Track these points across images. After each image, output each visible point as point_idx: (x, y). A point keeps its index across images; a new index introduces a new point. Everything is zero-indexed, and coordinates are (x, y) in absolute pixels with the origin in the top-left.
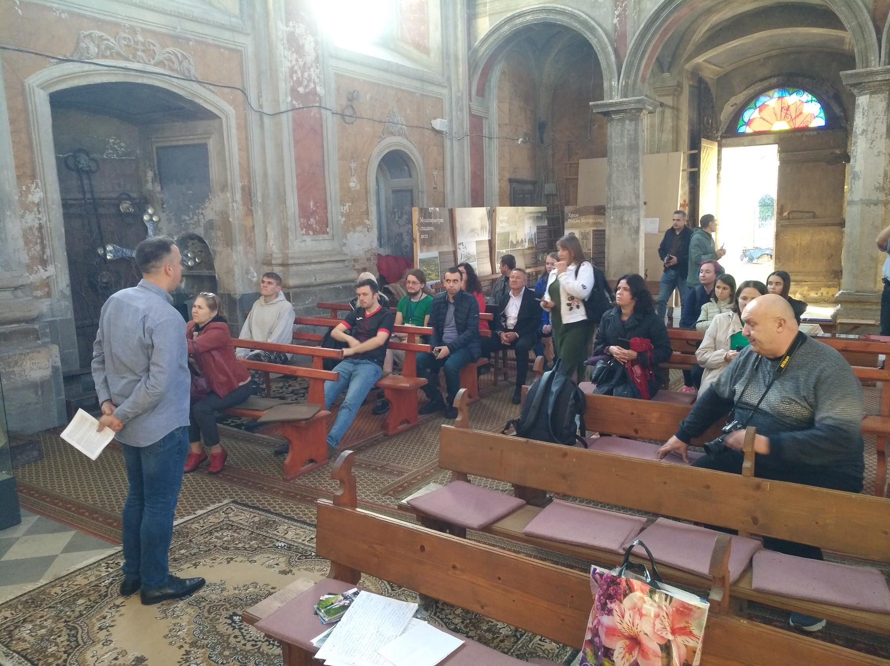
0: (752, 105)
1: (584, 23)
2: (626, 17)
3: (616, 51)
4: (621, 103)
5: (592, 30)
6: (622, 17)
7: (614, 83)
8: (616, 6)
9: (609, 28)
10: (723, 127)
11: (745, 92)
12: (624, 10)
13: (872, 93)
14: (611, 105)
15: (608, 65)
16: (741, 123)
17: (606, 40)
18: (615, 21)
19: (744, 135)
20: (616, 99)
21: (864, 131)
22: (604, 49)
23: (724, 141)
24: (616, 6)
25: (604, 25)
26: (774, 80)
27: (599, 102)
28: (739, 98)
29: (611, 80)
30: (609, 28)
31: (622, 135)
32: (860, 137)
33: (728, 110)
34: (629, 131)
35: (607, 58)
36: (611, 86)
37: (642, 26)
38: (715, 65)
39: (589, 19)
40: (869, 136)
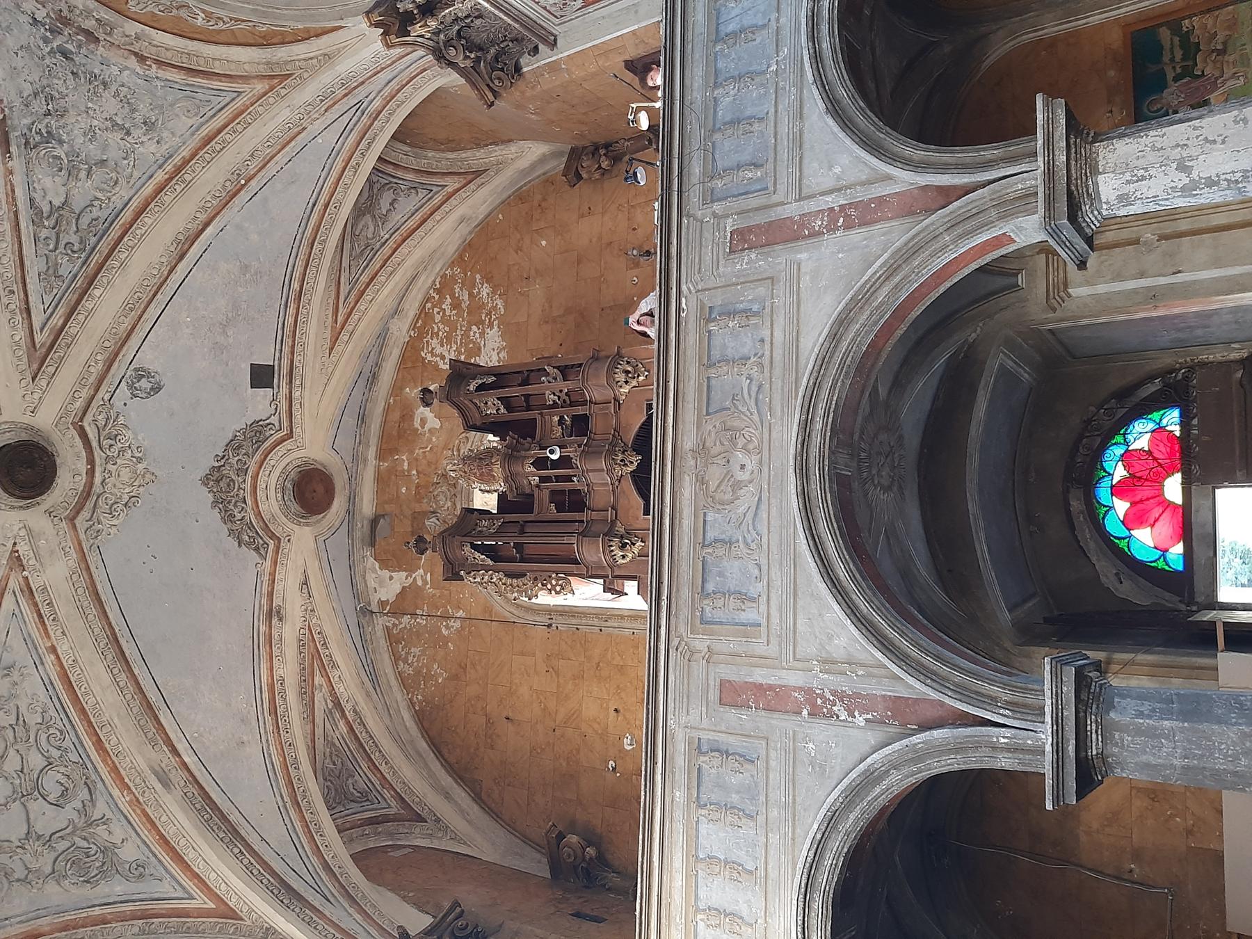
0: (1123, 544)
1: (854, 794)
2: (857, 695)
3: (925, 727)
4: (1058, 722)
5: (870, 779)
6: (854, 703)
7: (1002, 737)
8: (831, 715)
9: (872, 737)
10: (1169, 600)
11: (1094, 559)
12: (840, 696)
13: (1095, 171)
14: (1059, 748)
15: (957, 750)
16: (1161, 564)
17: (897, 746)
18: (860, 720)
19: (1188, 555)
20: (1045, 735)
21: (1183, 168)
22: (918, 756)
23: (1200, 599)
24: (831, 715)
25: (866, 748)
26: (1076, 505)
27: (1049, 782)
28: (1106, 570)
29: (995, 747)
30: (872, 737)
31: (1152, 733)
32: (1195, 175)
33: (1129, 590)
34: (1140, 714)
35: (944, 752)
36: (1011, 749)
37: (879, 655)
38: (1025, 601)
39: (846, 781)
40: (1194, 152)
